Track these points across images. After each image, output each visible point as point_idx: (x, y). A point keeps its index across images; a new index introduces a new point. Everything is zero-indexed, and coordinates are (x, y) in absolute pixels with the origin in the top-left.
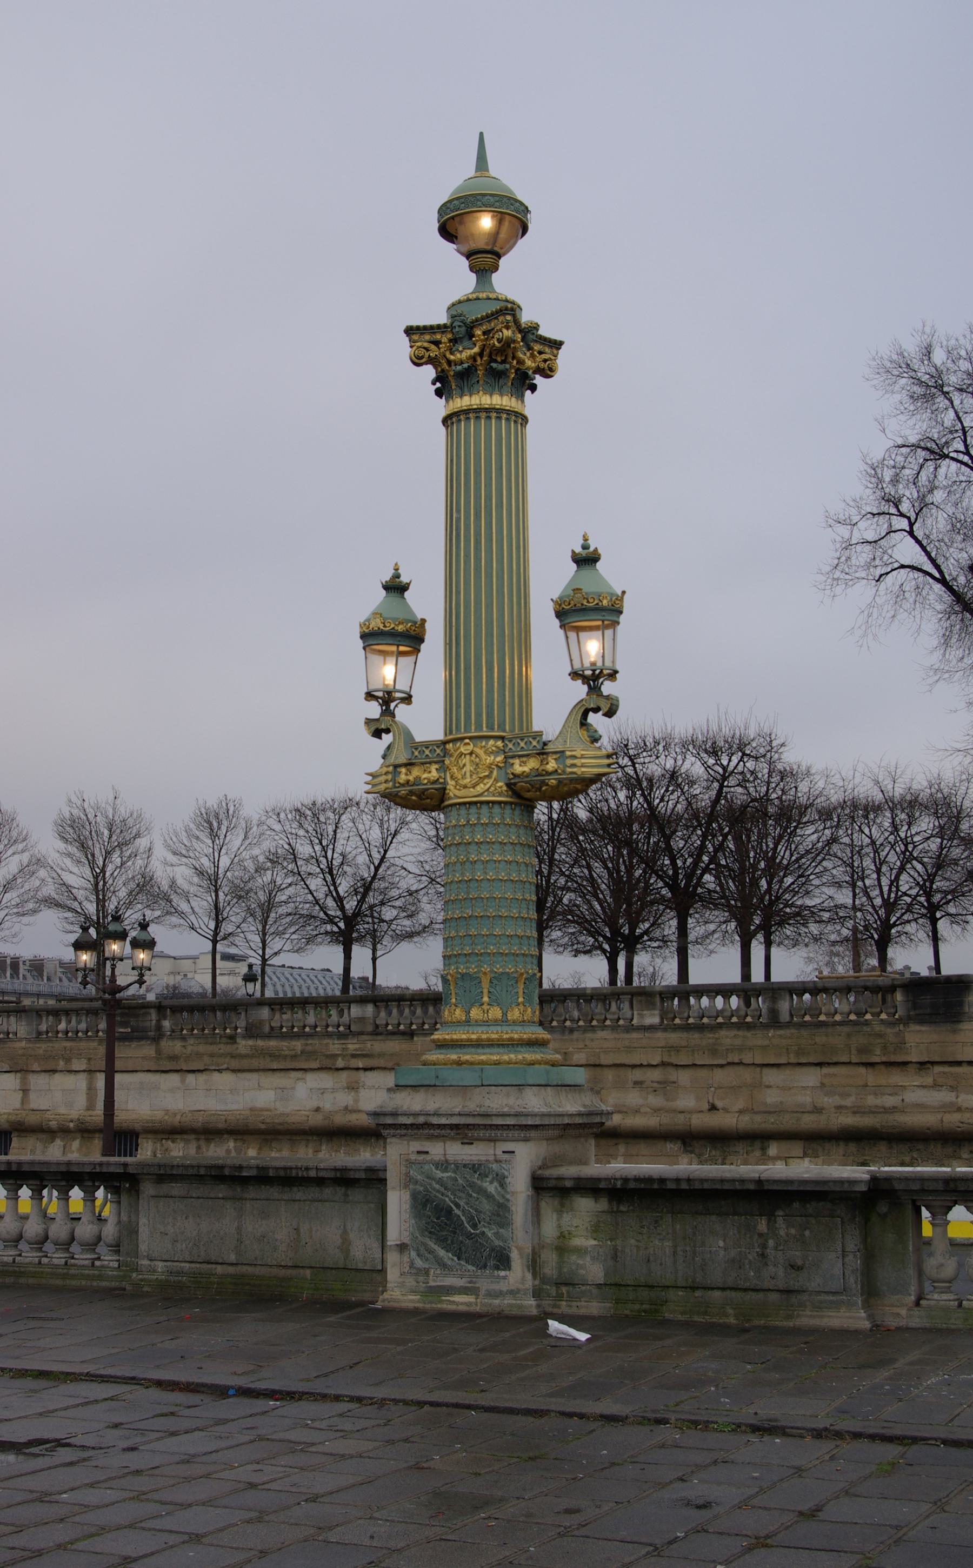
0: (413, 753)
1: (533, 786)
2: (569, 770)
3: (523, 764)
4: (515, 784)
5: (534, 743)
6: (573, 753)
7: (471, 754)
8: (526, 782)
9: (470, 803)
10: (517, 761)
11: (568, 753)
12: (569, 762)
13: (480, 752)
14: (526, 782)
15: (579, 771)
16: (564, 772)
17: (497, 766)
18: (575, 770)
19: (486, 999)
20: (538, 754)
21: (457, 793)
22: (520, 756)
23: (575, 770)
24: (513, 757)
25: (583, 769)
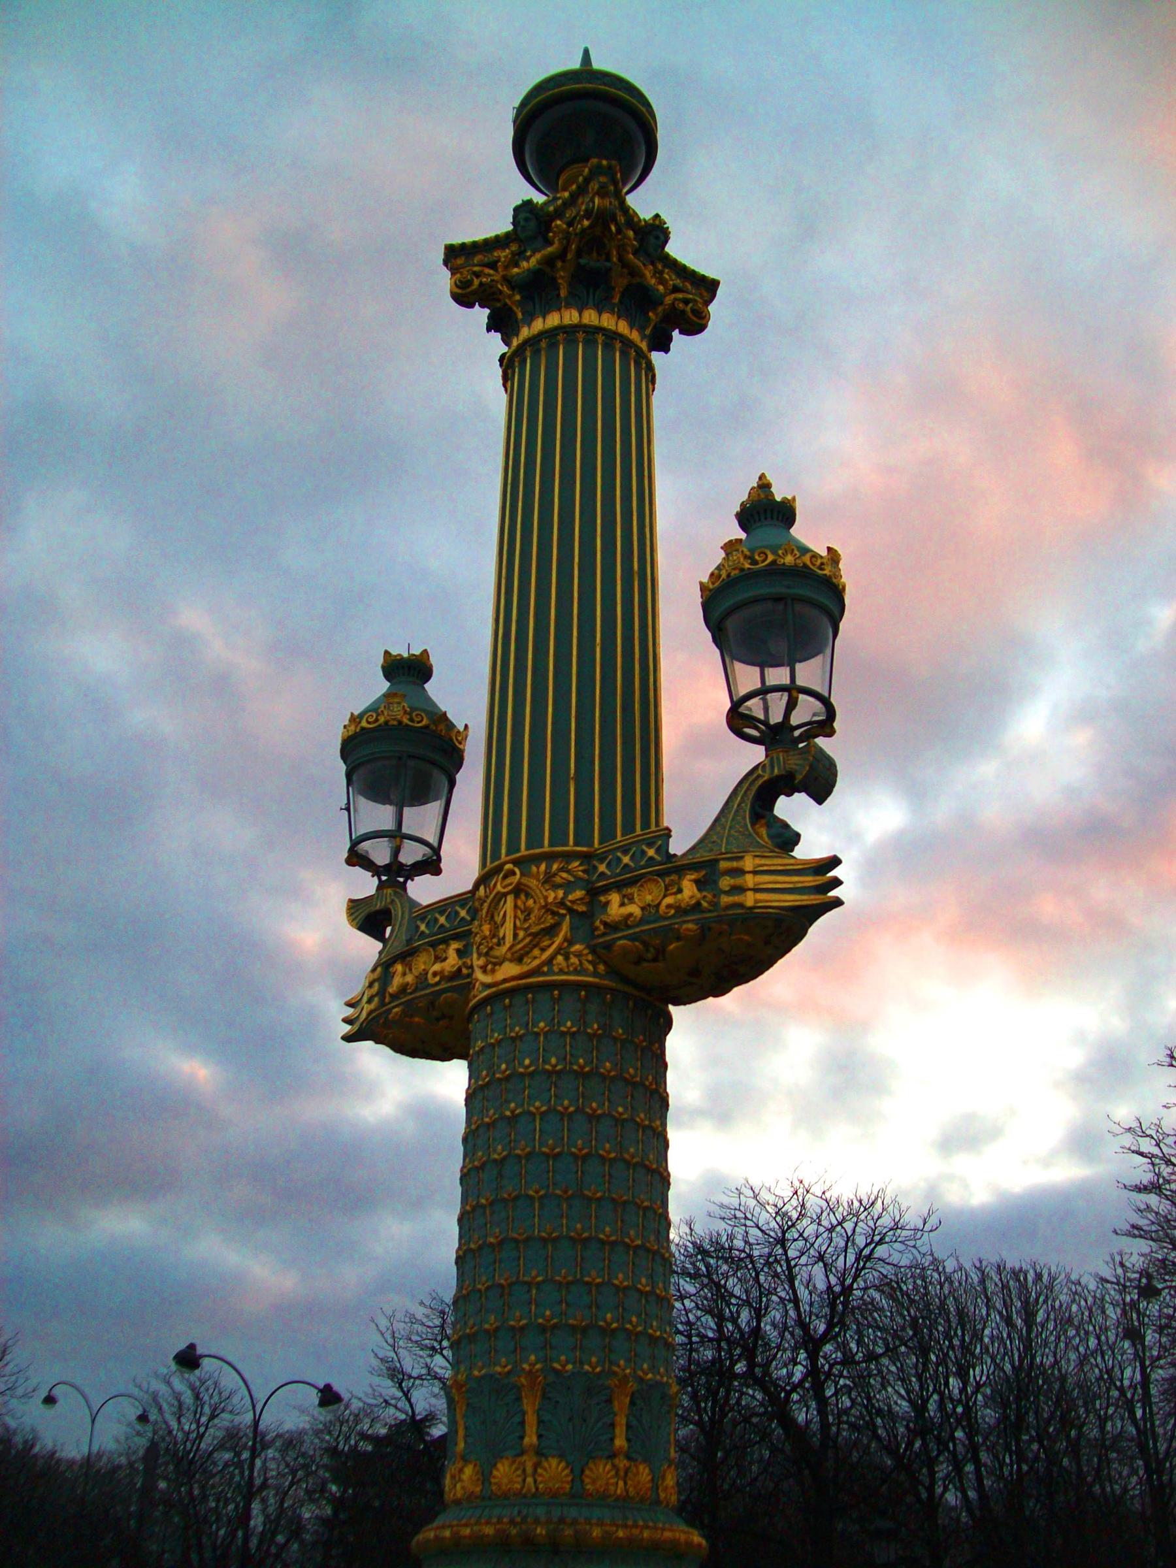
0: (418, 927)
1: (645, 943)
2: (725, 900)
3: (627, 899)
4: (608, 946)
5: (651, 852)
6: (735, 864)
7: (518, 890)
8: (632, 938)
9: (511, 992)
10: (615, 898)
11: (723, 865)
12: (725, 883)
13: (533, 883)
14: (632, 938)
15: (750, 899)
16: (715, 904)
17: (570, 911)
18: (736, 899)
19: (531, 1439)
20: (660, 874)
21: (487, 979)
22: (619, 886)
23: (736, 899)
24: (606, 890)
25: (760, 896)
